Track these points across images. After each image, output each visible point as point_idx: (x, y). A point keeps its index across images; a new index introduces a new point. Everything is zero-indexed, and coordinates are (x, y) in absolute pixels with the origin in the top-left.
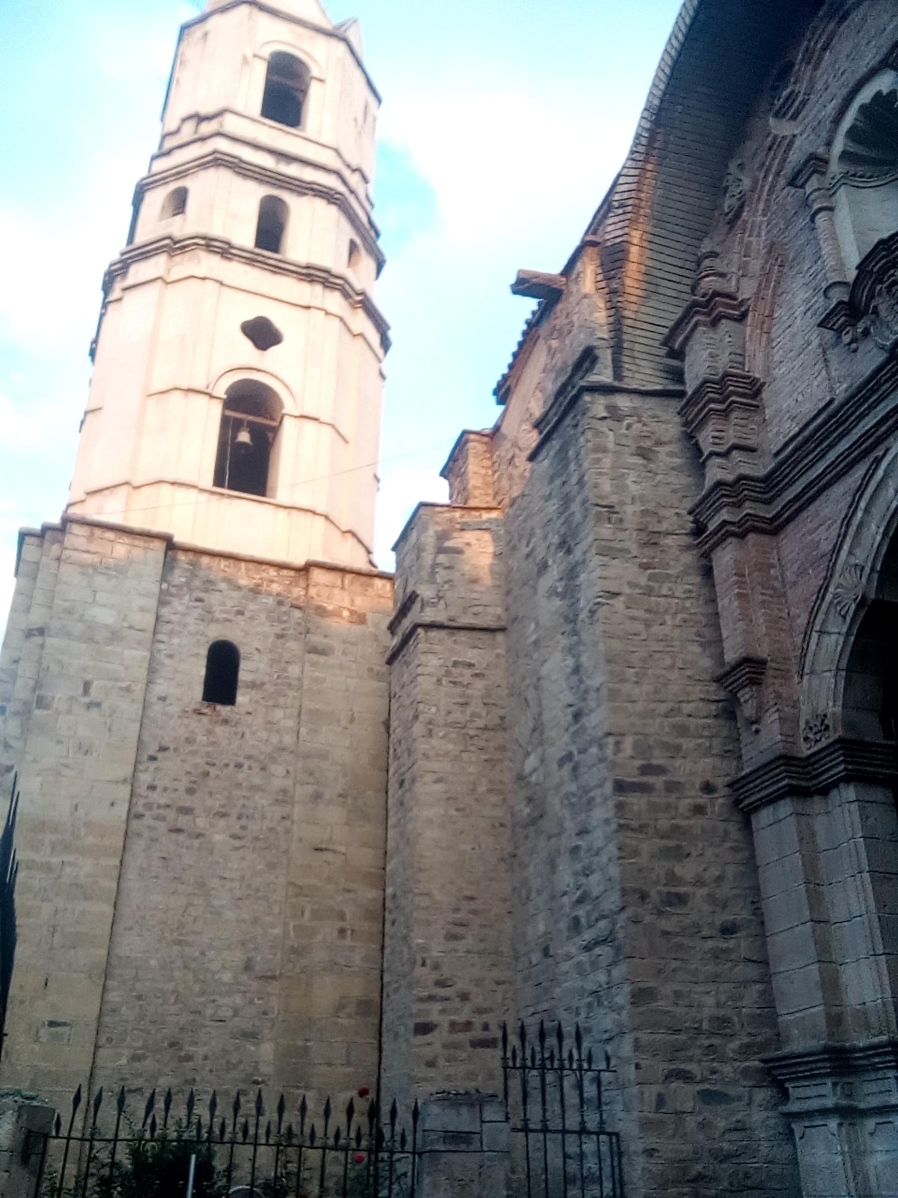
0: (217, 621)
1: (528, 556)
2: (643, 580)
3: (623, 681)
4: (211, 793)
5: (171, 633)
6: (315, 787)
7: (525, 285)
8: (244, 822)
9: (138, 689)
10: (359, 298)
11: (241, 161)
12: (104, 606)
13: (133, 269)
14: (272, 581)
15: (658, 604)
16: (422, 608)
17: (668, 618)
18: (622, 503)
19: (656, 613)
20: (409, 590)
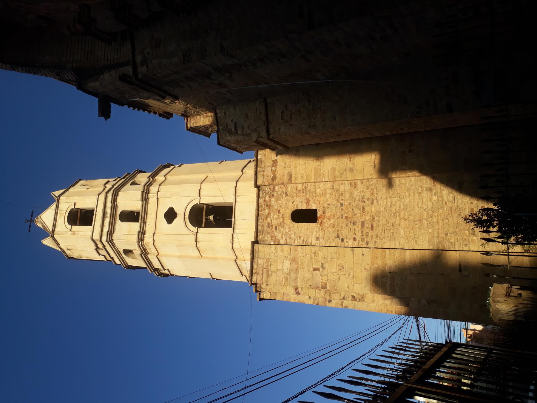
4: (355, 215)
5: (290, 238)
6: (348, 172)
7: (105, 113)
8: (365, 200)
9: (314, 249)
10: (151, 178)
11: (108, 232)
13: (156, 267)
14: (265, 201)
16: (262, 137)
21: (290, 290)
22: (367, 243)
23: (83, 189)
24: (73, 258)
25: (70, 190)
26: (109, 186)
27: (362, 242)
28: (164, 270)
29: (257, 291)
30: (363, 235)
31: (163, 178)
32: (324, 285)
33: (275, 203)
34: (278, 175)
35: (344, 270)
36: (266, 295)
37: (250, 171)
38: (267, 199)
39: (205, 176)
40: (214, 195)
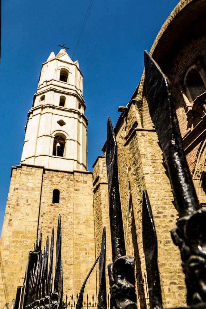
0: (55, 185)
1: (123, 167)
2: (153, 171)
3: (151, 193)
4: (55, 223)
6: (78, 221)
7: (120, 110)
10: (81, 115)
12: (30, 183)
13: (34, 112)
14: (66, 175)
15: (157, 175)
16: (101, 179)
17: (160, 178)
18: (147, 154)
19: (157, 177)
20: (97, 176)
21: (17, 186)
23: (78, 78)
24: (42, 67)
25: (79, 72)
26: (79, 92)
28: (33, 116)
29: (18, 167)
30: (44, 227)
33: (64, 181)
34: (79, 184)
35: (27, 216)
36: (14, 172)
37: (81, 169)
38: (66, 176)
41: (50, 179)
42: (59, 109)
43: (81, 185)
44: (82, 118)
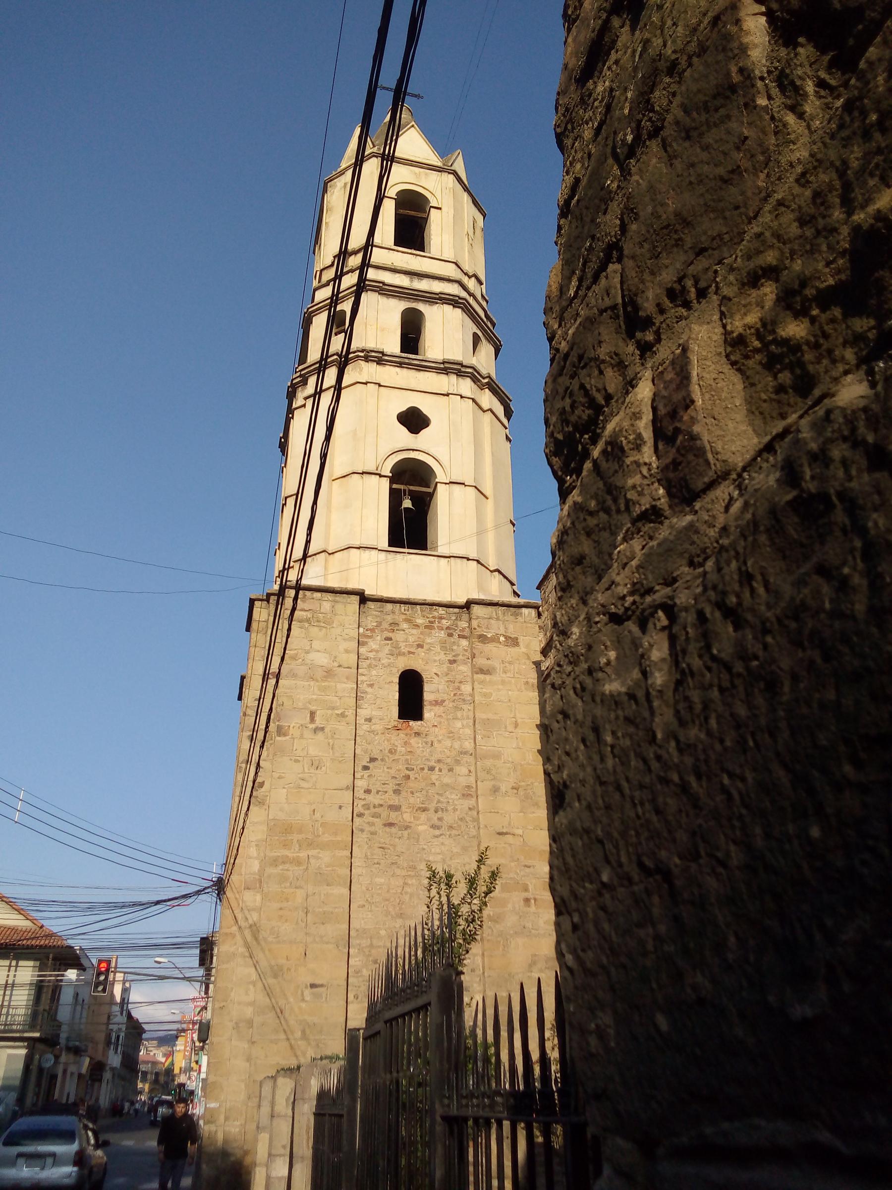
0: (401, 654)
4: (412, 793)
6: (493, 783)
8: (440, 814)
9: (350, 713)
10: (486, 380)
12: (319, 651)
14: (441, 618)
22: (360, 815)
23: (467, 226)
24: (325, 191)
25: (466, 195)
26: (471, 284)
27: (363, 806)
30: (374, 807)
31: (486, 406)
32: (283, 731)
34: (490, 648)
35: (312, 771)
37: (497, 590)
38: (444, 621)
39: (487, 494)
40: (451, 514)
41: (387, 634)
42: (400, 365)
43: (497, 653)
44: (487, 390)
